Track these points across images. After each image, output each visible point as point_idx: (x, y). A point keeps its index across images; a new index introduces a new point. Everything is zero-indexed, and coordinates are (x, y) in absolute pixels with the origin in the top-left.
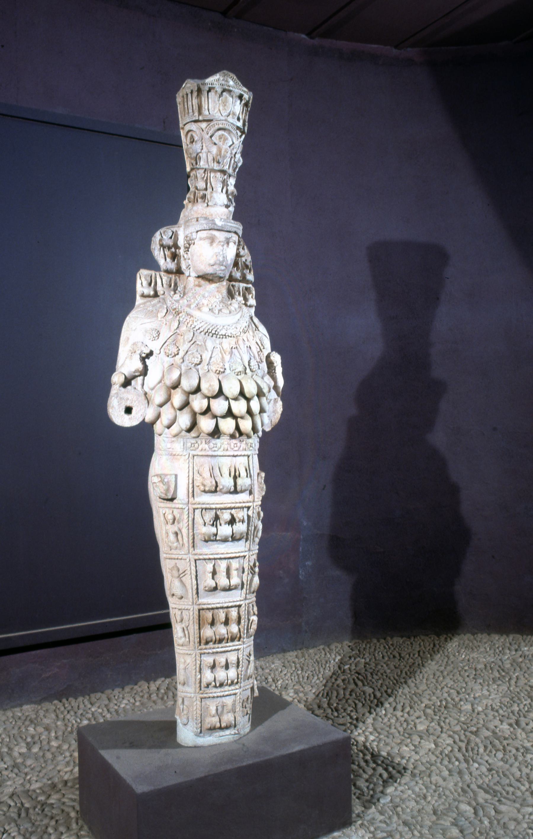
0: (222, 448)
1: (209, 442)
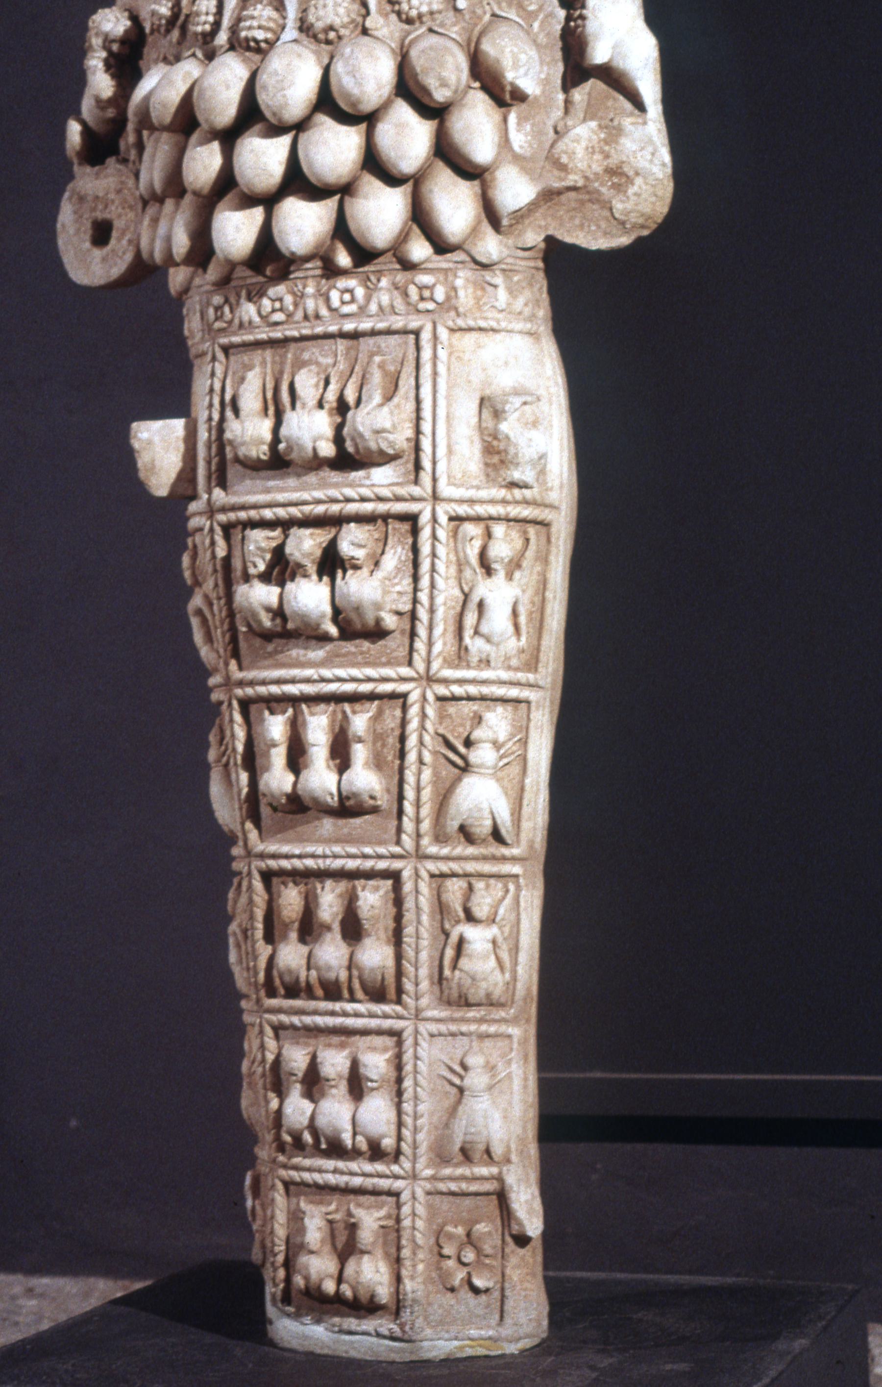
0: (299, 315)
1: (262, 294)
